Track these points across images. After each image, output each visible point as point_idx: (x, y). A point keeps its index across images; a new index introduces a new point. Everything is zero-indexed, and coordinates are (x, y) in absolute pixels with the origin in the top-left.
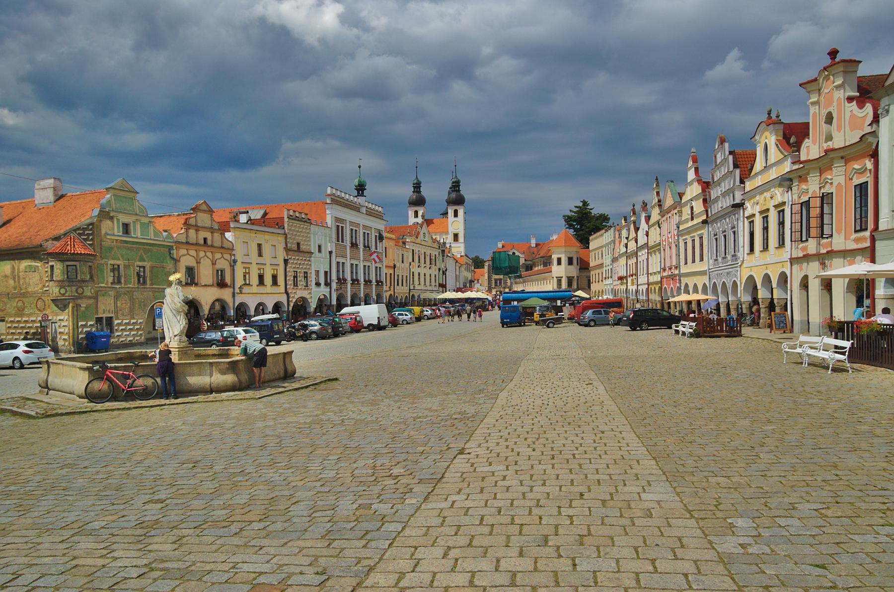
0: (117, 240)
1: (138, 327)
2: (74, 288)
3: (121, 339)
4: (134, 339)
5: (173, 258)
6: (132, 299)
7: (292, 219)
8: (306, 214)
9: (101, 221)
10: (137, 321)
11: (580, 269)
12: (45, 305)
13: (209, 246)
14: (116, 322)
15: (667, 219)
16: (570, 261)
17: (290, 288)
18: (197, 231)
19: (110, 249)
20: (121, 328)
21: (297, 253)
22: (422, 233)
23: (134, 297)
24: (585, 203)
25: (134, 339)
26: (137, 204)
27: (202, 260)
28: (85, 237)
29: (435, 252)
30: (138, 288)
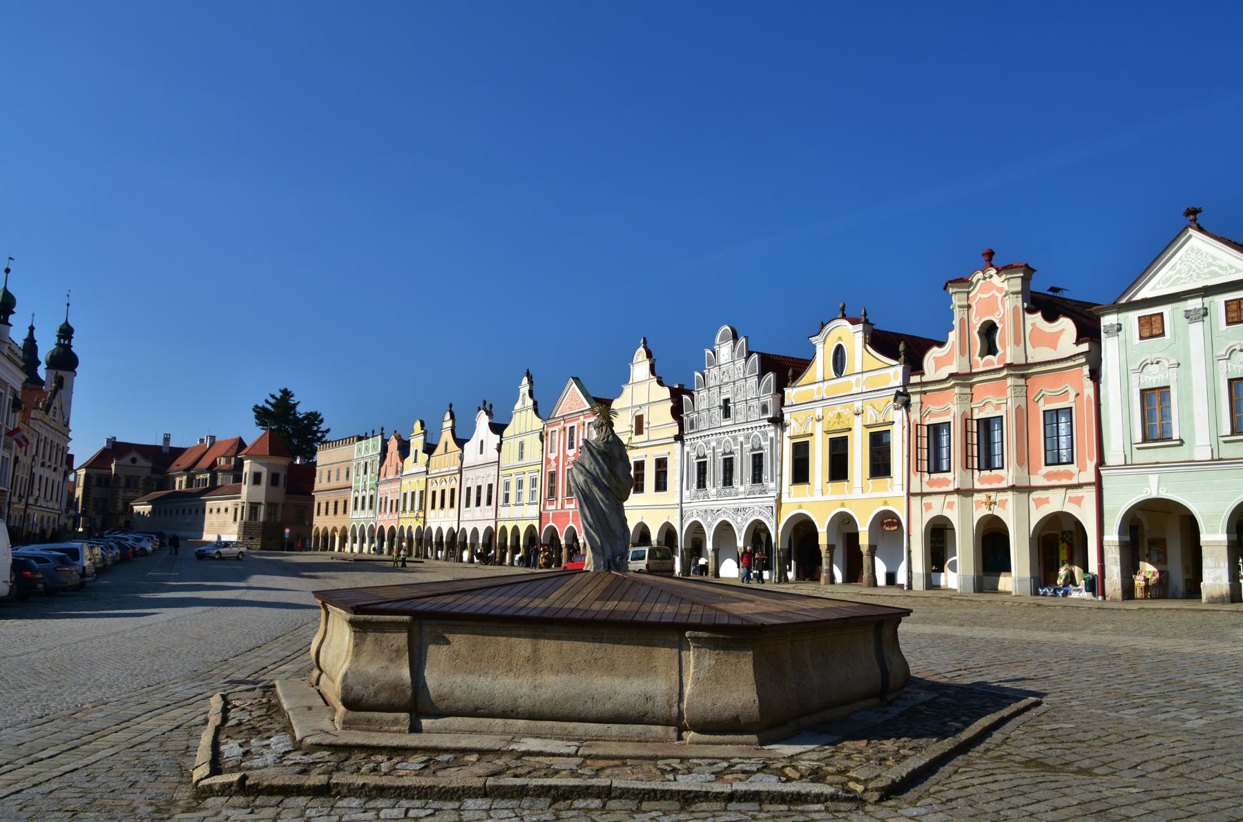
11: (287, 492)
15: (565, 429)
16: (274, 480)
24: (286, 394)
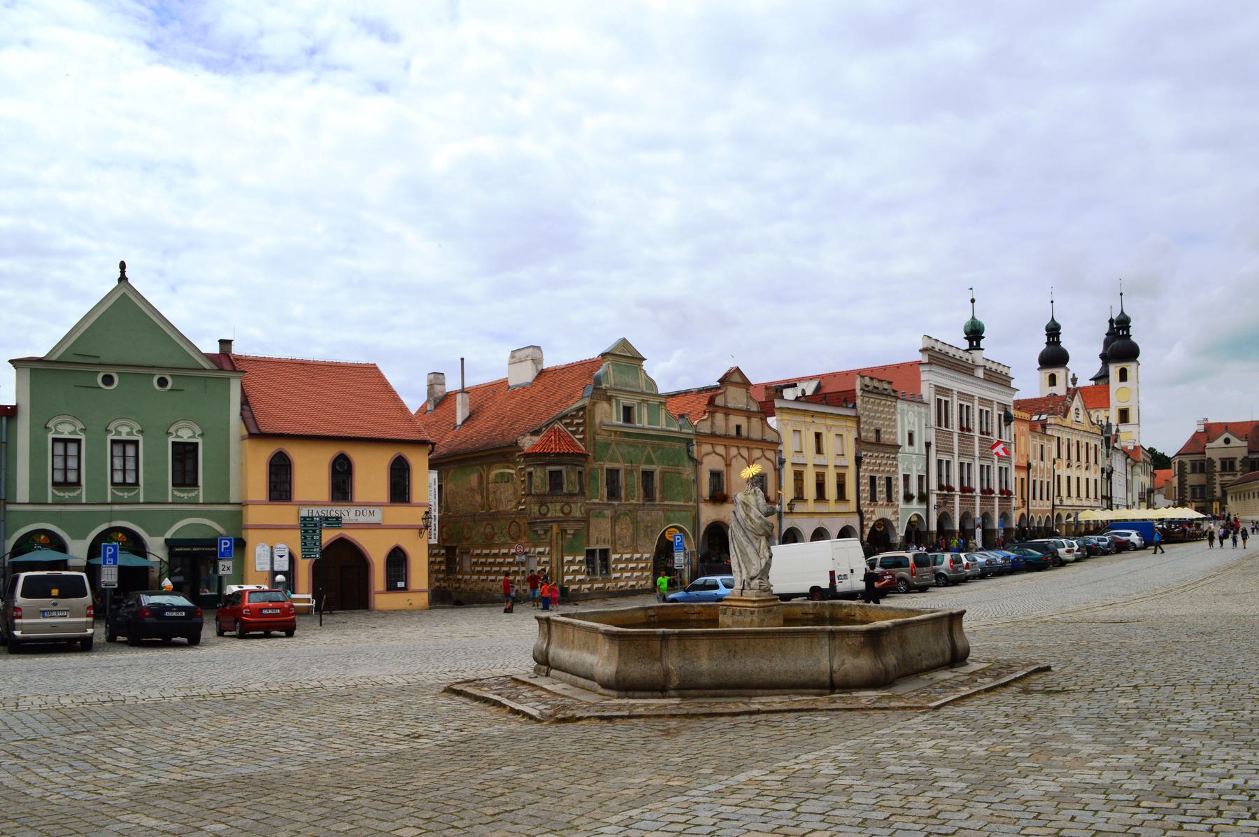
0: (616, 432)
1: (643, 565)
2: (558, 506)
3: (620, 584)
4: (637, 583)
5: (691, 459)
6: (635, 523)
7: (869, 392)
8: (890, 383)
9: (595, 404)
10: (642, 556)
12: (520, 531)
13: (744, 439)
14: (614, 557)
17: (864, 504)
18: (727, 415)
19: (607, 445)
21: (874, 448)
22: (1072, 410)
23: (638, 519)
26: (643, 376)
27: (734, 461)
28: (574, 429)
29: (1095, 441)
30: (644, 505)
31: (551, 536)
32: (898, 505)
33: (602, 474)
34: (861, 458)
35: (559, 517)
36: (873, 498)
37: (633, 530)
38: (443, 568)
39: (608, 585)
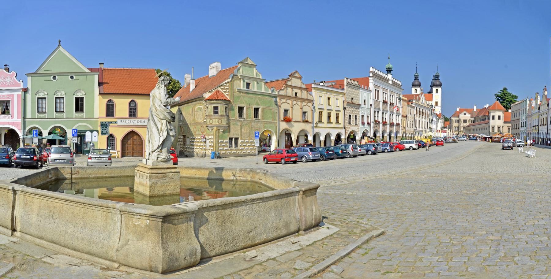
2: (217, 120)
3: (243, 151)
4: (251, 151)
19: (239, 97)
20: (243, 144)
22: (421, 99)
23: (252, 126)
25: (251, 151)
27: (294, 107)
31: (214, 131)
32: (359, 126)
33: (236, 108)
34: (345, 108)
35: (217, 124)
36: (350, 123)
37: (250, 130)
38: (182, 143)
39: (238, 152)
